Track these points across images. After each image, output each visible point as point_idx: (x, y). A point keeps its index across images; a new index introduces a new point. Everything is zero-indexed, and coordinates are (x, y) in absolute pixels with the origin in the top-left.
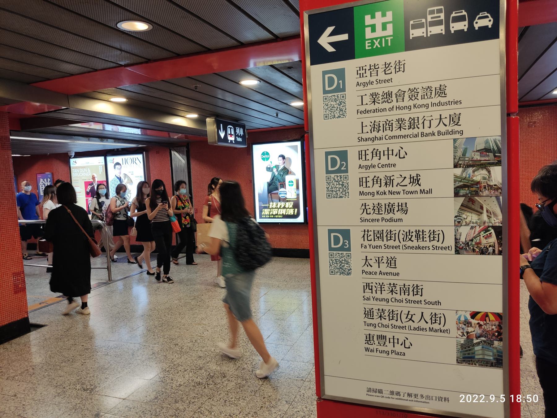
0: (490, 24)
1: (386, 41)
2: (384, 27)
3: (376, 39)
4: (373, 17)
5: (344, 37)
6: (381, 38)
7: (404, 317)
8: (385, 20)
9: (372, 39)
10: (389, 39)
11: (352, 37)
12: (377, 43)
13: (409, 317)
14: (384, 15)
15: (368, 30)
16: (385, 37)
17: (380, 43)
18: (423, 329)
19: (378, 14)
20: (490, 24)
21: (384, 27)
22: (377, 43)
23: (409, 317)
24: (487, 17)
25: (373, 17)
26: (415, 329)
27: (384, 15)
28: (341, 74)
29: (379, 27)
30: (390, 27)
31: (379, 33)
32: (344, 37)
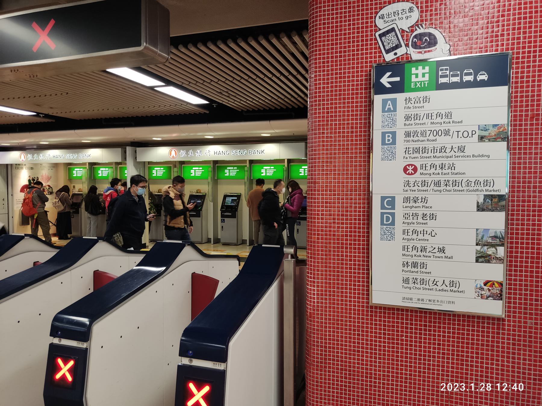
1: (424, 84)
3: (418, 82)
4: (417, 69)
6: (421, 82)
8: (424, 71)
9: (415, 82)
10: (426, 82)
12: (418, 85)
15: (413, 77)
16: (424, 81)
17: (421, 84)
22: (418, 85)
25: (417, 69)
28: (394, 101)
29: (420, 75)
30: (427, 76)
31: (420, 78)
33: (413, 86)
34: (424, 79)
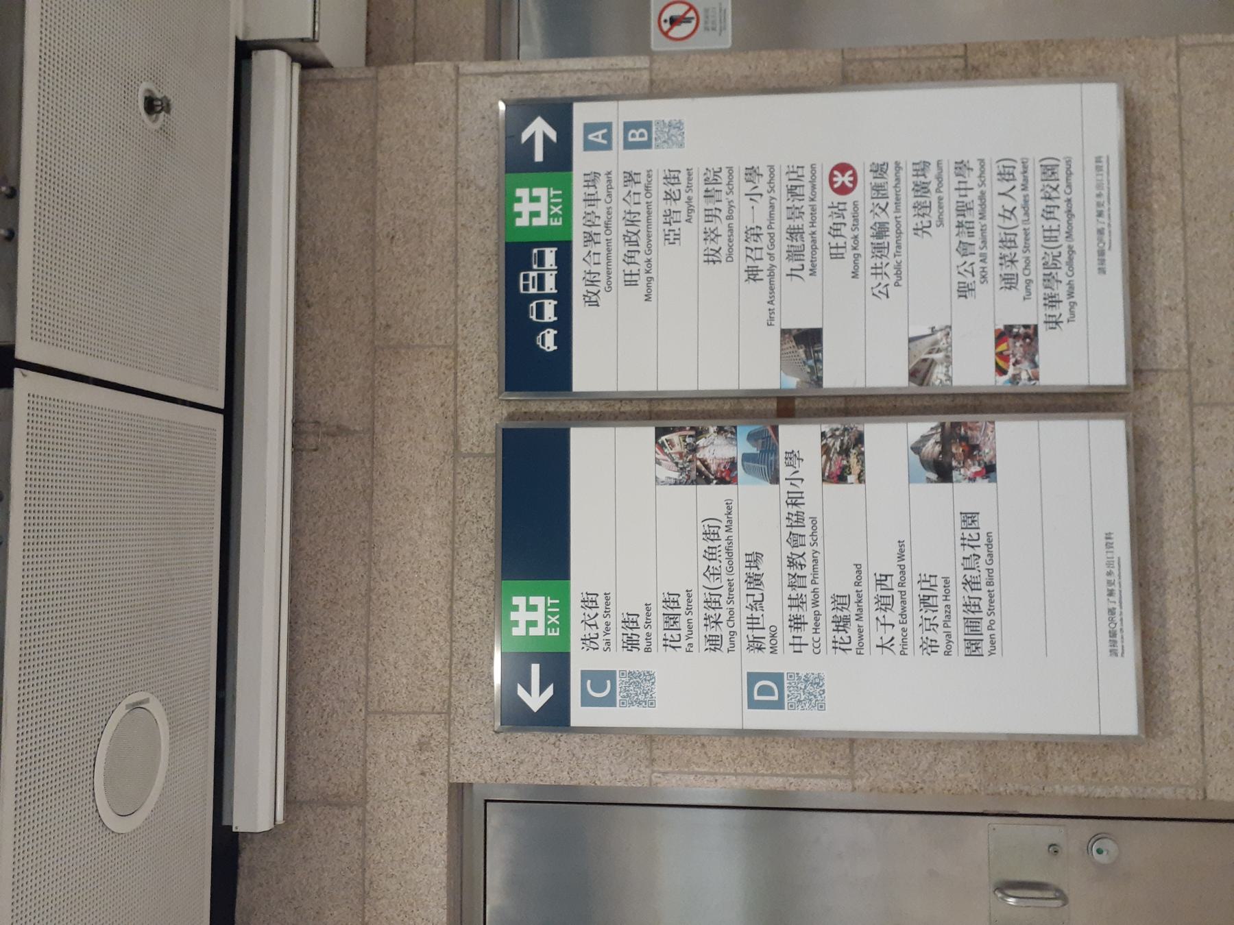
0: (553, 332)
2: (535, 199)
5: (539, 156)
7: (1008, 224)
11: (539, 168)
12: (556, 210)
13: (1007, 214)
14: (519, 200)
16: (549, 198)
17: (556, 205)
18: (1026, 201)
19: (517, 207)
20: (553, 332)
21: (535, 199)
22: (556, 210)
23: (1007, 214)
24: (543, 336)
26: (1027, 214)
27: (519, 200)
31: (542, 207)
32: (539, 156)
33: (557, 223)
34: (544, 199)
